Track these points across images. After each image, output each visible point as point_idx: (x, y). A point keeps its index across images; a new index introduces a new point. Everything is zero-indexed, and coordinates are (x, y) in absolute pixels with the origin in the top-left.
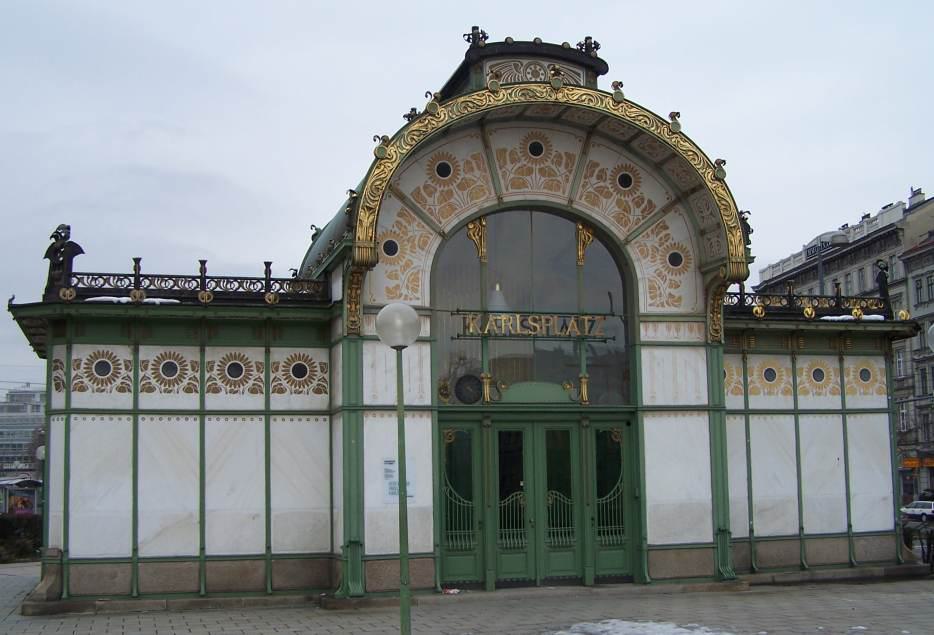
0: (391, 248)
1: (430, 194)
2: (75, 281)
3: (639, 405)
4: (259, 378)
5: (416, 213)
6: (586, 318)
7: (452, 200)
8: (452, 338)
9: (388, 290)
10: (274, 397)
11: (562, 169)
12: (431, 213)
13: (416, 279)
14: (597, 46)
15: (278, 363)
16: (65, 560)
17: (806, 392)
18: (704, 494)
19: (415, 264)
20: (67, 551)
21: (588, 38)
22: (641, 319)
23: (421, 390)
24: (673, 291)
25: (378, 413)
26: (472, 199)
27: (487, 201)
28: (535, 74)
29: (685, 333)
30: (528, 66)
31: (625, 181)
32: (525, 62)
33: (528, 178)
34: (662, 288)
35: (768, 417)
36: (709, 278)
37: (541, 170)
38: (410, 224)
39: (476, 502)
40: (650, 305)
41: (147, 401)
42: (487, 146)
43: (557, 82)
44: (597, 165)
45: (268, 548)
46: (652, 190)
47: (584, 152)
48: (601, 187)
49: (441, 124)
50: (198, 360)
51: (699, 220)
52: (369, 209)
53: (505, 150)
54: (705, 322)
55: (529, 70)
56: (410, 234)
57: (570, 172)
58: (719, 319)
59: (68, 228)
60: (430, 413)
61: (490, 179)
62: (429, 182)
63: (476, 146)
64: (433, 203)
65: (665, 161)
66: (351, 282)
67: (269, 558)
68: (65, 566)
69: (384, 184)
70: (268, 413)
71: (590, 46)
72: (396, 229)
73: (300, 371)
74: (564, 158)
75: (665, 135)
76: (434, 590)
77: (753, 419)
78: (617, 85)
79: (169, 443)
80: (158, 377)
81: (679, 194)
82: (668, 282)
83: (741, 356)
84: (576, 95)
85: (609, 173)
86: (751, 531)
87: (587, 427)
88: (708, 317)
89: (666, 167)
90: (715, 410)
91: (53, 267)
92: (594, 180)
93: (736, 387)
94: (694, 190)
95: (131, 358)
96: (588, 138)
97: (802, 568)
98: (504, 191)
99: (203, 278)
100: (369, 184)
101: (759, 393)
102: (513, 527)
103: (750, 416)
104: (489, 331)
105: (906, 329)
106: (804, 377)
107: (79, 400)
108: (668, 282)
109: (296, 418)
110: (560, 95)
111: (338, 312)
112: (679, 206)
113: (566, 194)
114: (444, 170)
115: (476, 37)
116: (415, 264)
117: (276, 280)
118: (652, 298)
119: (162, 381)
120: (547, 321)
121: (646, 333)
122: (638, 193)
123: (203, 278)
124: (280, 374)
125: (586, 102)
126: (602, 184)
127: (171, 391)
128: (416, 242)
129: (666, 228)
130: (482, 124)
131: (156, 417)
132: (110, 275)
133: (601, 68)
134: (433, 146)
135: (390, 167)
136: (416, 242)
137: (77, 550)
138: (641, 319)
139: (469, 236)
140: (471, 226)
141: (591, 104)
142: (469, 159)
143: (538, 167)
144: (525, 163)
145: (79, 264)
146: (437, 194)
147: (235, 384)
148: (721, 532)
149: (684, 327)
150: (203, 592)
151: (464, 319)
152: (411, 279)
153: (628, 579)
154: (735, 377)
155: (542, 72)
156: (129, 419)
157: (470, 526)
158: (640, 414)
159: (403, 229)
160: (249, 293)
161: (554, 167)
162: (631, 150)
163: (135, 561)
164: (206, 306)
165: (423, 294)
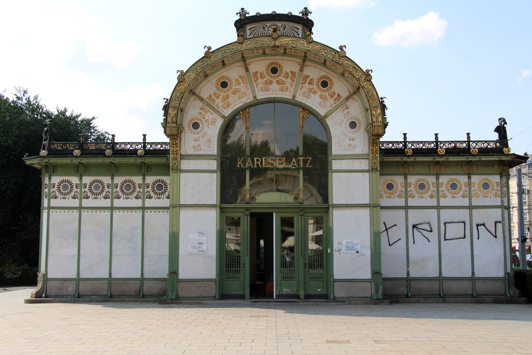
0: (196, 126)
1: (217, 98)
7: (229, 100)
9: (194, 147)
11: (289, 80)
12: (218, 108)
13: (210, 141)
17: (445, 196)
24: (351, 142)
25: (188, 208)
26: (240, 98)
31: (324, 84)
32: (268, 25)
33: (270, 86)
34: (346, 142)
35: (420, 210)
40: (338, 150)
42: (247, 70)
43: (275, 35)
44: (308, 77)
46: (340, 87)
47: (301, 70)
49: (212, 62)
55: (270, 29)
56: (206, 118)
57: (293, 81)
60: (215, 208)
61: (249, 88)
62: (217, 91)
64: (219, 102)
72: (199, 116)
73: (160, 187)
74: (290, 74)
77: (410, 212)
80: (91, 191)
82: (348, 138)
83: (403, 176)
85: (315, 81)
86: (408, 274)
90: (374, 206)
92: (307, 85)
95: (78, 182)
98: (257, 94)
103: (409, 210)
107: (54, 203)
112: (355, 96)
113: (292, 94)
117: (149, 143)
121: (336, 165)
122: (332, 91)
126: (311, 87)
128: (210, 122)
129: (348, 108)
136: (210, 122)
138: (333, 158)
140: (241, 113)
141: (294, 46)
142: (239, 79)
143: (276, 80)
144: (269, 78)
146: (221, 97)
147: (128, 194)
148: (376, 273)
149: (357, 162)
154: (400, 188)
158: (331, 209)
161: (284, 79)
162: (327, 68)
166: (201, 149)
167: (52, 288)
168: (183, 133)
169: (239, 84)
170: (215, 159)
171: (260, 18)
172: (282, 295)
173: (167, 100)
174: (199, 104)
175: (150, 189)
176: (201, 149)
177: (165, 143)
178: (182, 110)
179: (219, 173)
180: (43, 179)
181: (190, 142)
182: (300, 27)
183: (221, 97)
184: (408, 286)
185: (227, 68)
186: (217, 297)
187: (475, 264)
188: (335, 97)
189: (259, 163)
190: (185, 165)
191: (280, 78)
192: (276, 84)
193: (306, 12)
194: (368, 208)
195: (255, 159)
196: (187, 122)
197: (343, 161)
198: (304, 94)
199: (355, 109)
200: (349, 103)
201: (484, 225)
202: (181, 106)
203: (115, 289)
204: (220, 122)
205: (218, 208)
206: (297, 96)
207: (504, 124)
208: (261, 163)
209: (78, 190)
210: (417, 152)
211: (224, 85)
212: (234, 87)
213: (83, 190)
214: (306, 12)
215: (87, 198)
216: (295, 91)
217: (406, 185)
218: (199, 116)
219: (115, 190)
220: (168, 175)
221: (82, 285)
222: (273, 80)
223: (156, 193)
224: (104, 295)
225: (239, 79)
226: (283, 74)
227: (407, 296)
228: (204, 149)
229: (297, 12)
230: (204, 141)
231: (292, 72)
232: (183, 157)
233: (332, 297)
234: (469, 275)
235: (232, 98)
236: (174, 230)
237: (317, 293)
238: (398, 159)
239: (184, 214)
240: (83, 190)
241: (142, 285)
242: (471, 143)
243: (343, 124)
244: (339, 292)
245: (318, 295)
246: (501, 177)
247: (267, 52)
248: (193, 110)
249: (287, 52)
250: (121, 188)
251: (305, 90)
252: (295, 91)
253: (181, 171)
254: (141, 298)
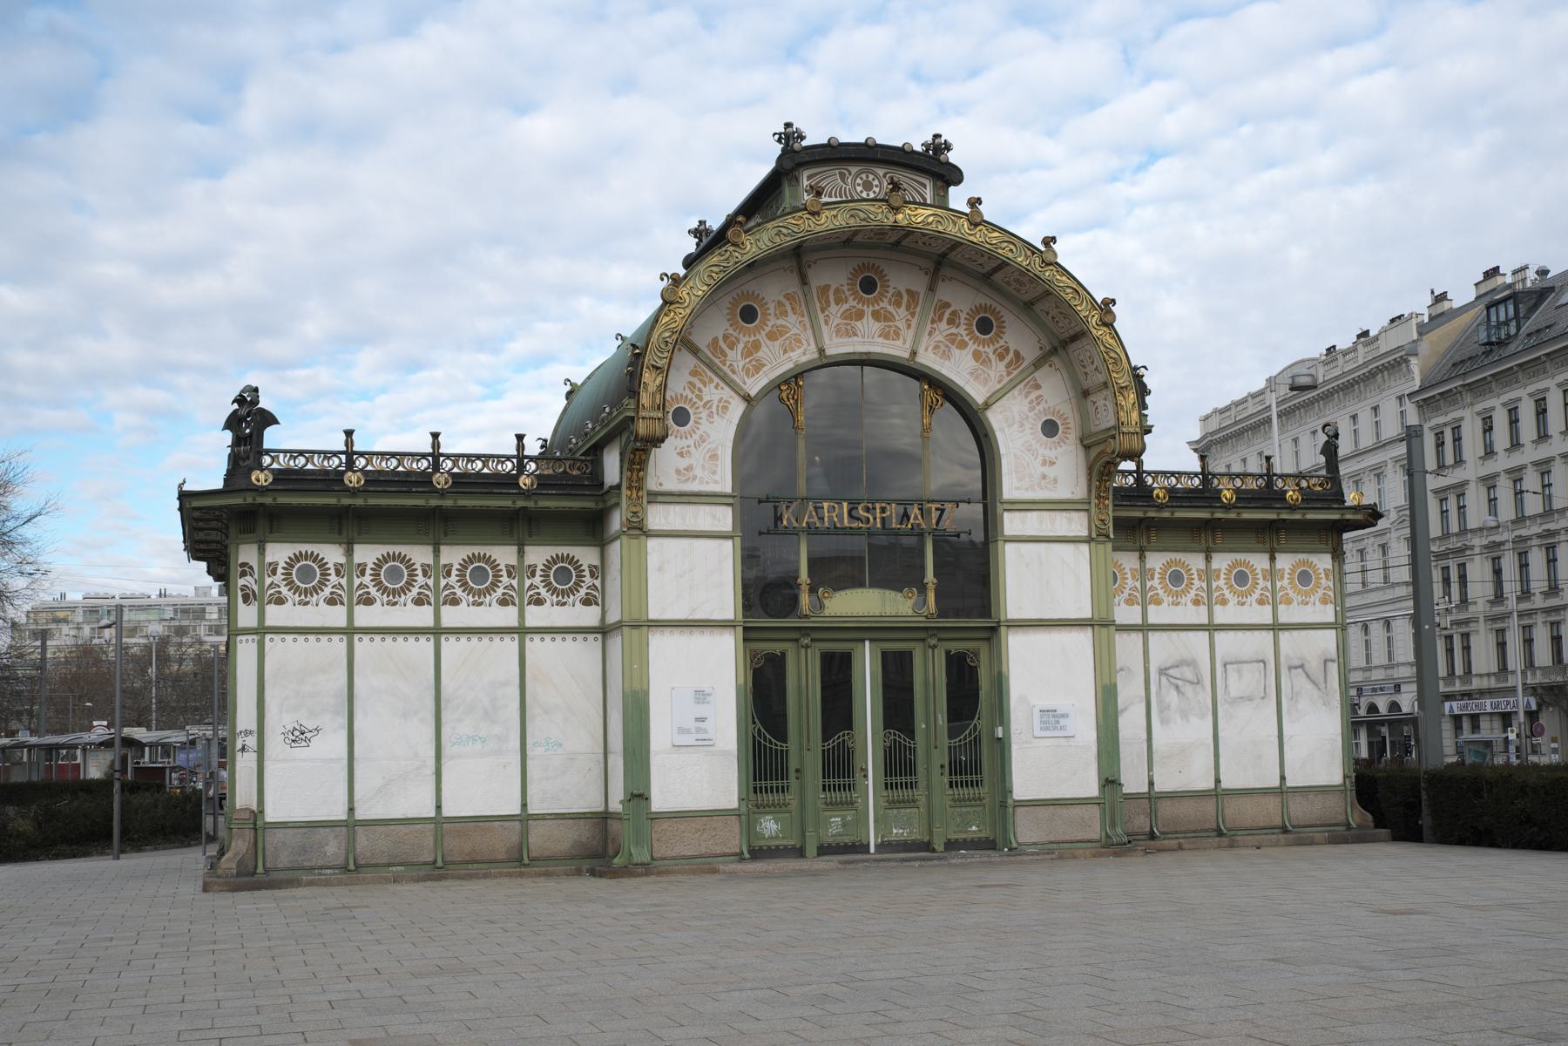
0: (682, 417)
2: (267, 460)
5: (717, 374)
6: (934, 506)
7: (760, 354)
8: (761, 533)
9: (678, 472)
11: (902, 311)
13: (714, 457)
14: (948, 147)
16: (259, 823)
17: (1224, 602)
20: (262, 812)
21: (937, 136)
24: (1046, 470)
25: (667, 630)
26: (785, 352)
28: (868, 186)
30: (858, 175)
32: (854, 170)
33: (859, 324)
35: (1174, 634)
36: (1094, 452)
39: (792, 745)
42: (804, 281)
44: (947, 305)
46: (1020, 338)
50: (431, 562)
51: (1082, 378)
53: (826, 288)
57: (913, 315)
59: (256, 390)
63: (793, 285)
64: (735, 358)
65: (1038, 299)
66: (632, 462)
68: (260, 832)
71: (939, 147)
72: (687, 392)
74: (905, 298)
75: (1035, 265)
76: (740, 857)
77: (1154, 637)
78: (974, 202)
79: (394, 670)
80: (378, 584)
81: (1056, 344)
84: (920, 216)
85: (963, 316)
86: (1151, 784)
89: (1038, 307)
90: (1100, 624)
91: (238, 441)
92: (943, 325)
94: (1075, 338)
95: (342, 560)
96: (937, 270)
98: (827, 341)
99: (436, 456)
100: (655, 335)
105: (1359, 517)
107: (276, 615)
109: (559, 637)
110: (900, 216)
111: (613, 501)
112: (1055, 359)
113: (908, 344)
114: (749, 315)
115: (789, 136)
119: (385, 590)
120: (883, 510)
121: (1012, 523)
122: (1002, 343)
123: (436, 456)
126: (954, 330)
129: (1038, 387)
130: (797, 258)
131: (377, 638)
132: (313, 452)
133: (949, 176)
135: (679, 315)
137: (271, 815)
139: (781, 400)
141: (940, 228)
145: (272, 438)
146: (741, 346)
148: (1110, 782)
150: (440, 863)
151: (776, 508)
153: (988, 845)
154: (1130, 581)
155: (876, 182)
156: (341, 640)
157: (784, 774)
158: (1003, 629)
160: (497, 475)
161: (891, 309)
163: (351, 825)
164: (442, 494)
169: (785, 314)
172: (890, 844)
175: (537, 580)
176: (695, 478)
179: (738, 540)
180: (232, 549)
182: (927, 182)
183: (741, 346)
184: (1152, 814)
187: (1286, 757)
190: (657, 517)
194: (1090, 629)
195: (826, 505)
197: (1029, 514)
198: (936, 347)
199: (1053, 392)
200: (1039, 375)
201: (1302, 666)
203: (456, 847)
205: (740, 630)
206: (921, 351)
208: (840, 517)
209: (344, 581)
213: (357, 582)
215: (369, 601)
216: (916, 340)
217: (1144, 574)
218: (687, 392)
219: (443, 582)
221: (363, 840)
223: (554, 591)
224: (426, 864)
227: (1152, 836)
230: (701, 453)
231: (909, 292)
234: (1276, 783)
236: (636, 686)
237: (969, 836)
239: (660, 644)
240: (357, 582)
241: (525, 833)
243: (1028, 426)
244: (1026, 830)
245: (972, 840)
250: (462, 575)
251: (940, 338)
252: (916, 340)
253: (649, 534)
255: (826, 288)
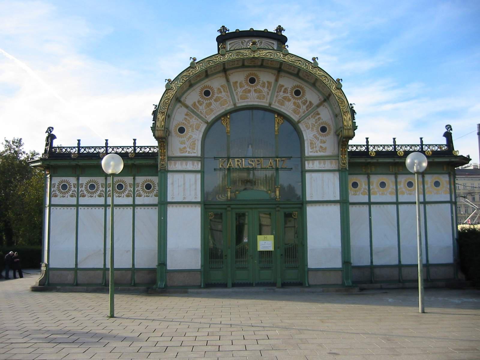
0: (182, 130)
1: (201, 105)
3: (304, 200)
4: (131, 190)
5: (194, 114)
6: (278, 159)
7: (212, 107)
9: (180, 149)
10: (137, 198)
11: (266, 89)
12: (202, 113)
15: (139, 183)
17: (403, 193)
18: (337, 243)
19: (193, 137)
22: (306, 159)
23: (196, 194)
24: (322, 145)
25: (174, 205)
27: (229, 106)
29: (328, 165)
30: (248, 42)
31: (297, 93)
32: (247, 40)
33: (249, 94)
34: (316, 144)
35: (382, 206)
37: (255, 90)
38: (191, 119)
40: (311, 152)
41: (82, 201)
42: (228, 81)
44: (283, 86)
45: (133, 265)
46: (312, 96)
47: (277, 80)
48: (285, 96)
49: (197, 72)
50: (104, 183)
52: (162, 113)
54: (338, 159)
56: (191, 123)
57: (270, 90)
58: (345, 158)
61: (230, 96)
62: (200, 99)
64: (202, 108)
67: (133, 270)
69: (169, 101)
70: (134, 206)
72: (184, 121)
73: (148, 187)
77: (373, 207)
81: (325, 98)
82: (320, 140)
83: (366, 176)
85: (289, 90)
87: (279, 211)
88: (340, 157)
93: (364, 191)
95: (76, 183)
97: (399, 281)
98: (237, 101)
101: (377, 194)
102: (214, 259)
104: (229, 166)
106: (402, 185)
107: (55, 201)
108: (320, 140)
109: (146, 207)
112: (325, 104)
113: (268, 101)
115: (223, 29)
116: (193, 137)
118: (312, 149)
119: (89, 192)
121: (309, 166)
124: (139, 188)
125: (269, 56)
126: (286, 95)
127: (65, 196)
129: (318, 114)
131: (86, 208)
134: (203, 82)
141: (272, 57)
142: (220, 88)
145: (56, 143)
146: (204, 104)
148: (346, 262)
152: (191, 144)
153: (300, 284)
154: (363, 186)
158: (304, 204)
159: (188, 121)
161: (261, 88)
162: (300, 78)
163: (76, 270)
165: (197, 150)
166: (186, 151)
167: (54, 278)
168: (170, 138)
169: (221, 92)
170: (199, 160)
171: (239, 35)
173: (156, 106)
174: (184, 110)
176: (186, 151)
177: (154, 147)
178: (169, 116)
181: (177, 145)
183: (204, 104)
185: (209, 78)
186: (202, 286)
188: (307, 104)
189: (239, 163)
190: (173, 166)
191: (258, 87)
192: (254, 93)
193: (280, 29)
196: (173, 127)
199: (325, 115)
202: (169, 112)
204: (204, 127)
207: (450, 130)
210: (379, 154)
211: (207, 93)
212: (216, 95)
214: (280, 29)
215: (84, 196)
216: (271, 98)
220: (156, 175)
222: (251, 89)
224: (100, 284)
225: (220, 88)
226: (260, 84)
228: (189, 152)
229: (272, 29)
230: (189, 143)
231: (268, 82)
232: (170, 158)
233: (307, 285)
235: (214, 106)
238: (362, 160)
242: (424, 146)
243: (315, 129)
244: (312, 279)
246: (450, 176)
247: (246, 64)
248: (179, 116)
249: (264, 64)
251: (280, 98)
254: (133, 286)
255: (236, 82)
